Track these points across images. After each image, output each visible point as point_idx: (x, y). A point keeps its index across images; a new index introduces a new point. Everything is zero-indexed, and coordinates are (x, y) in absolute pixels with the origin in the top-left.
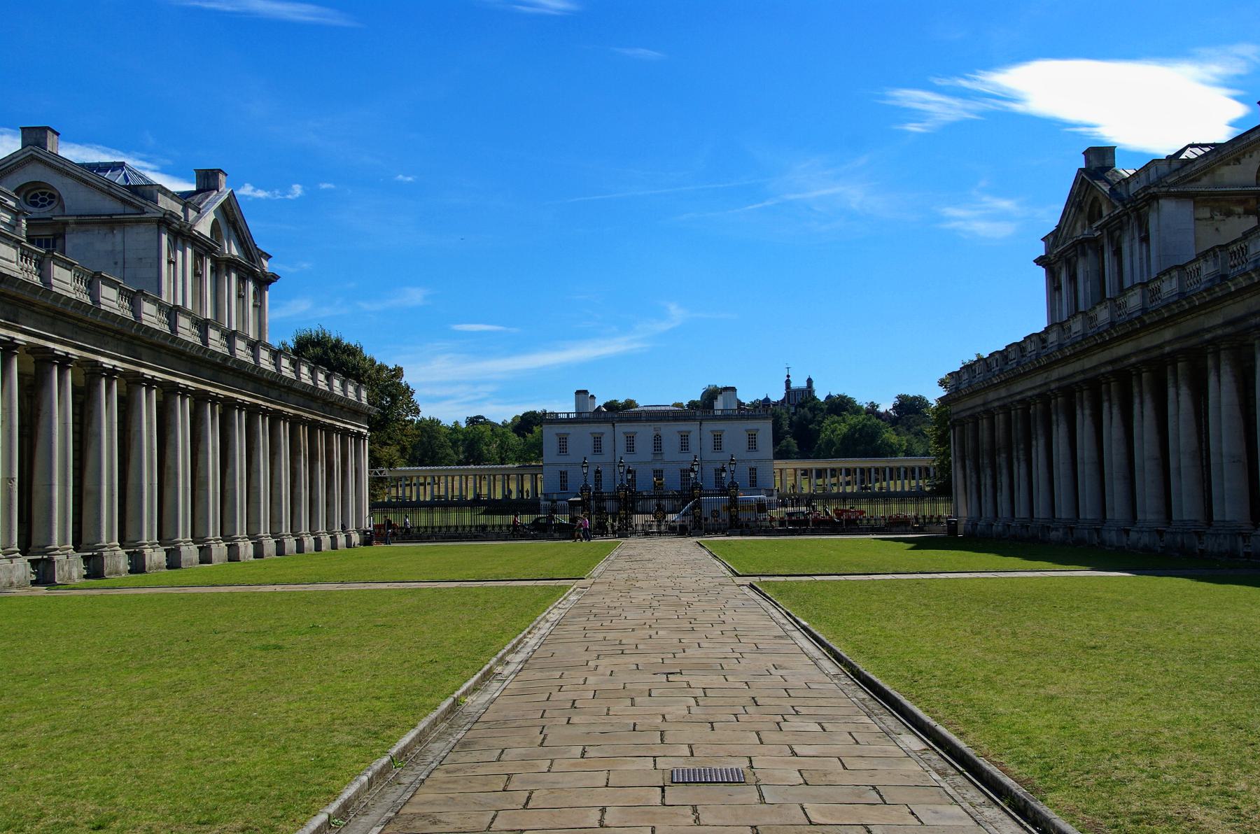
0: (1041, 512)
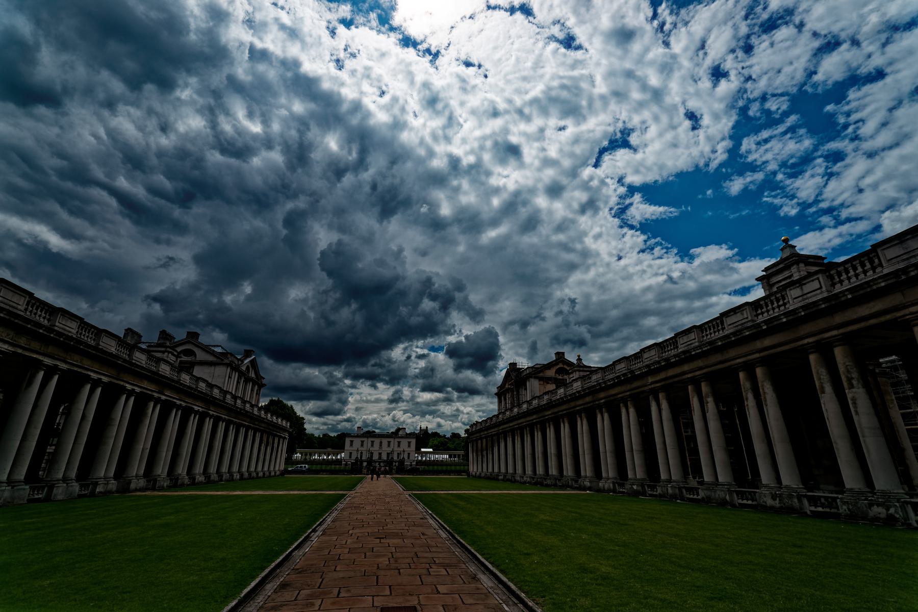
0: (496, 470)
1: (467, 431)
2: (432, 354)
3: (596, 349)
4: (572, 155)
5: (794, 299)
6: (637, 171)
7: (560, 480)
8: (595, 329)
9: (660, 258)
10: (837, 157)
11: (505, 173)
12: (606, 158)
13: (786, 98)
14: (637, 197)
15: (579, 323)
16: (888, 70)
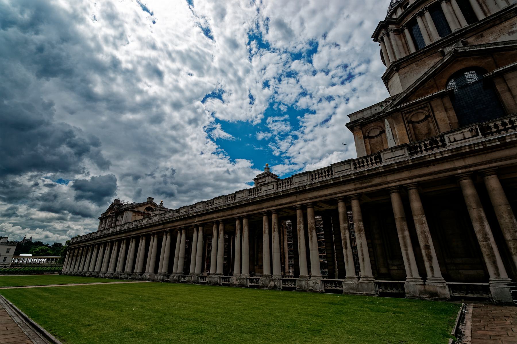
1: (68, 242)
2: (58, 185)
3: (176, 199)
4: (192, 91)
5: (264, 191)
6: (222, 113)
7: (130, 275)
8: (179, 188)
9: (221, 159)
10: (296, 137)
11: (149, 84)
12: (209, 100)
13: (286, 107)
14: (219, 126)
15: (172, 183)
16: (317, 112)
